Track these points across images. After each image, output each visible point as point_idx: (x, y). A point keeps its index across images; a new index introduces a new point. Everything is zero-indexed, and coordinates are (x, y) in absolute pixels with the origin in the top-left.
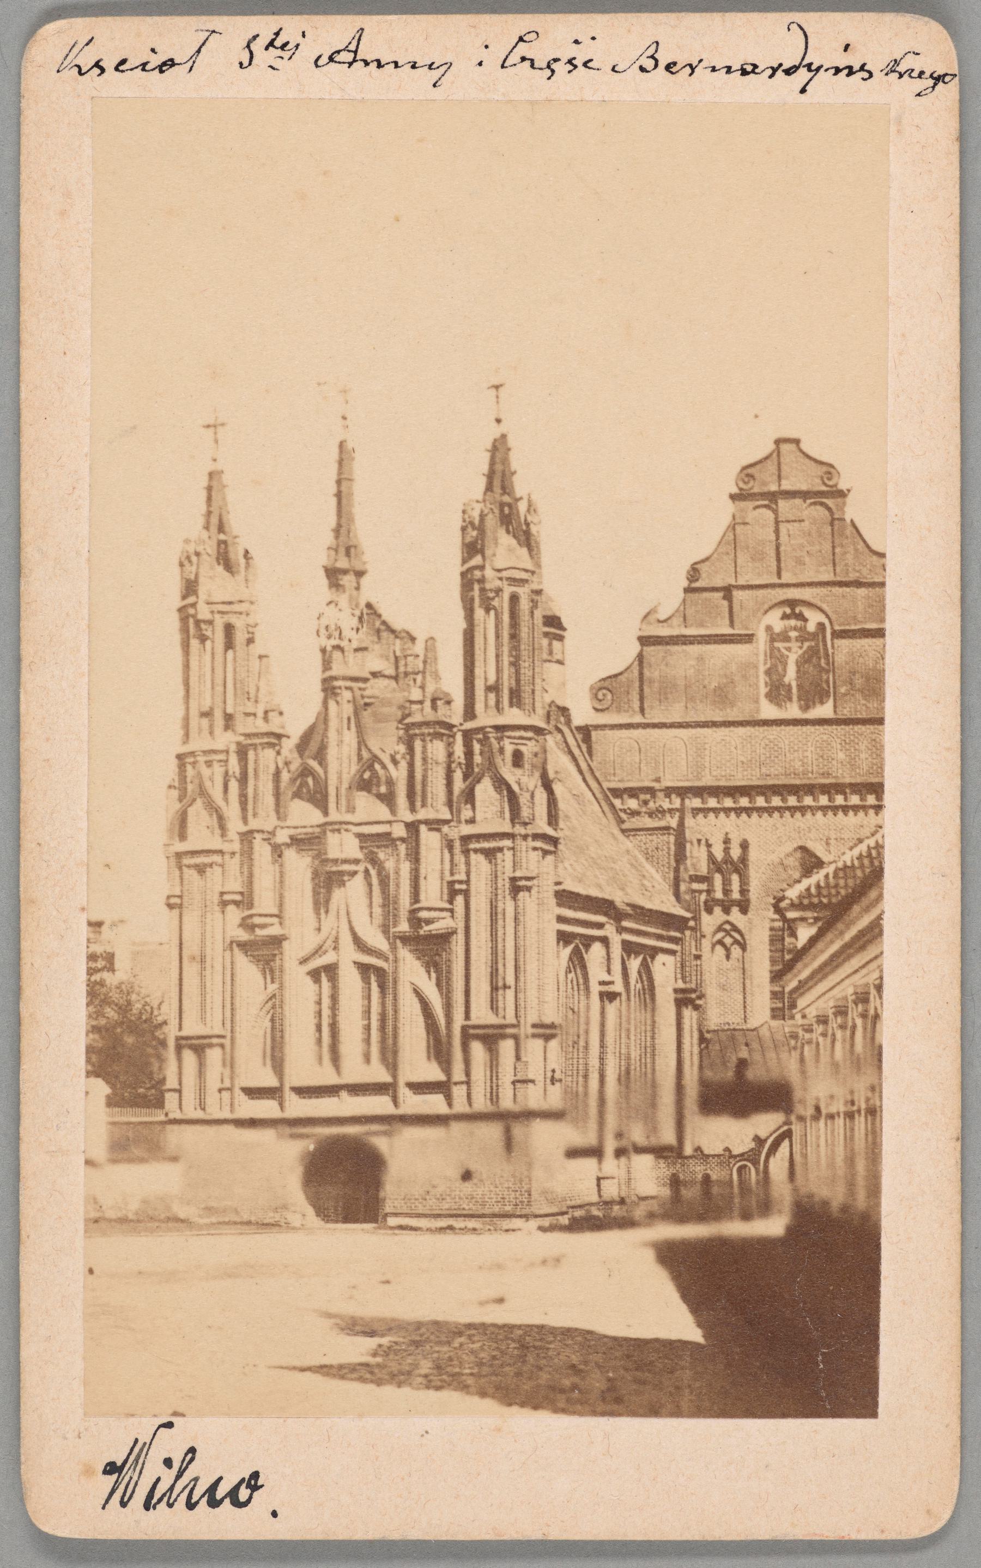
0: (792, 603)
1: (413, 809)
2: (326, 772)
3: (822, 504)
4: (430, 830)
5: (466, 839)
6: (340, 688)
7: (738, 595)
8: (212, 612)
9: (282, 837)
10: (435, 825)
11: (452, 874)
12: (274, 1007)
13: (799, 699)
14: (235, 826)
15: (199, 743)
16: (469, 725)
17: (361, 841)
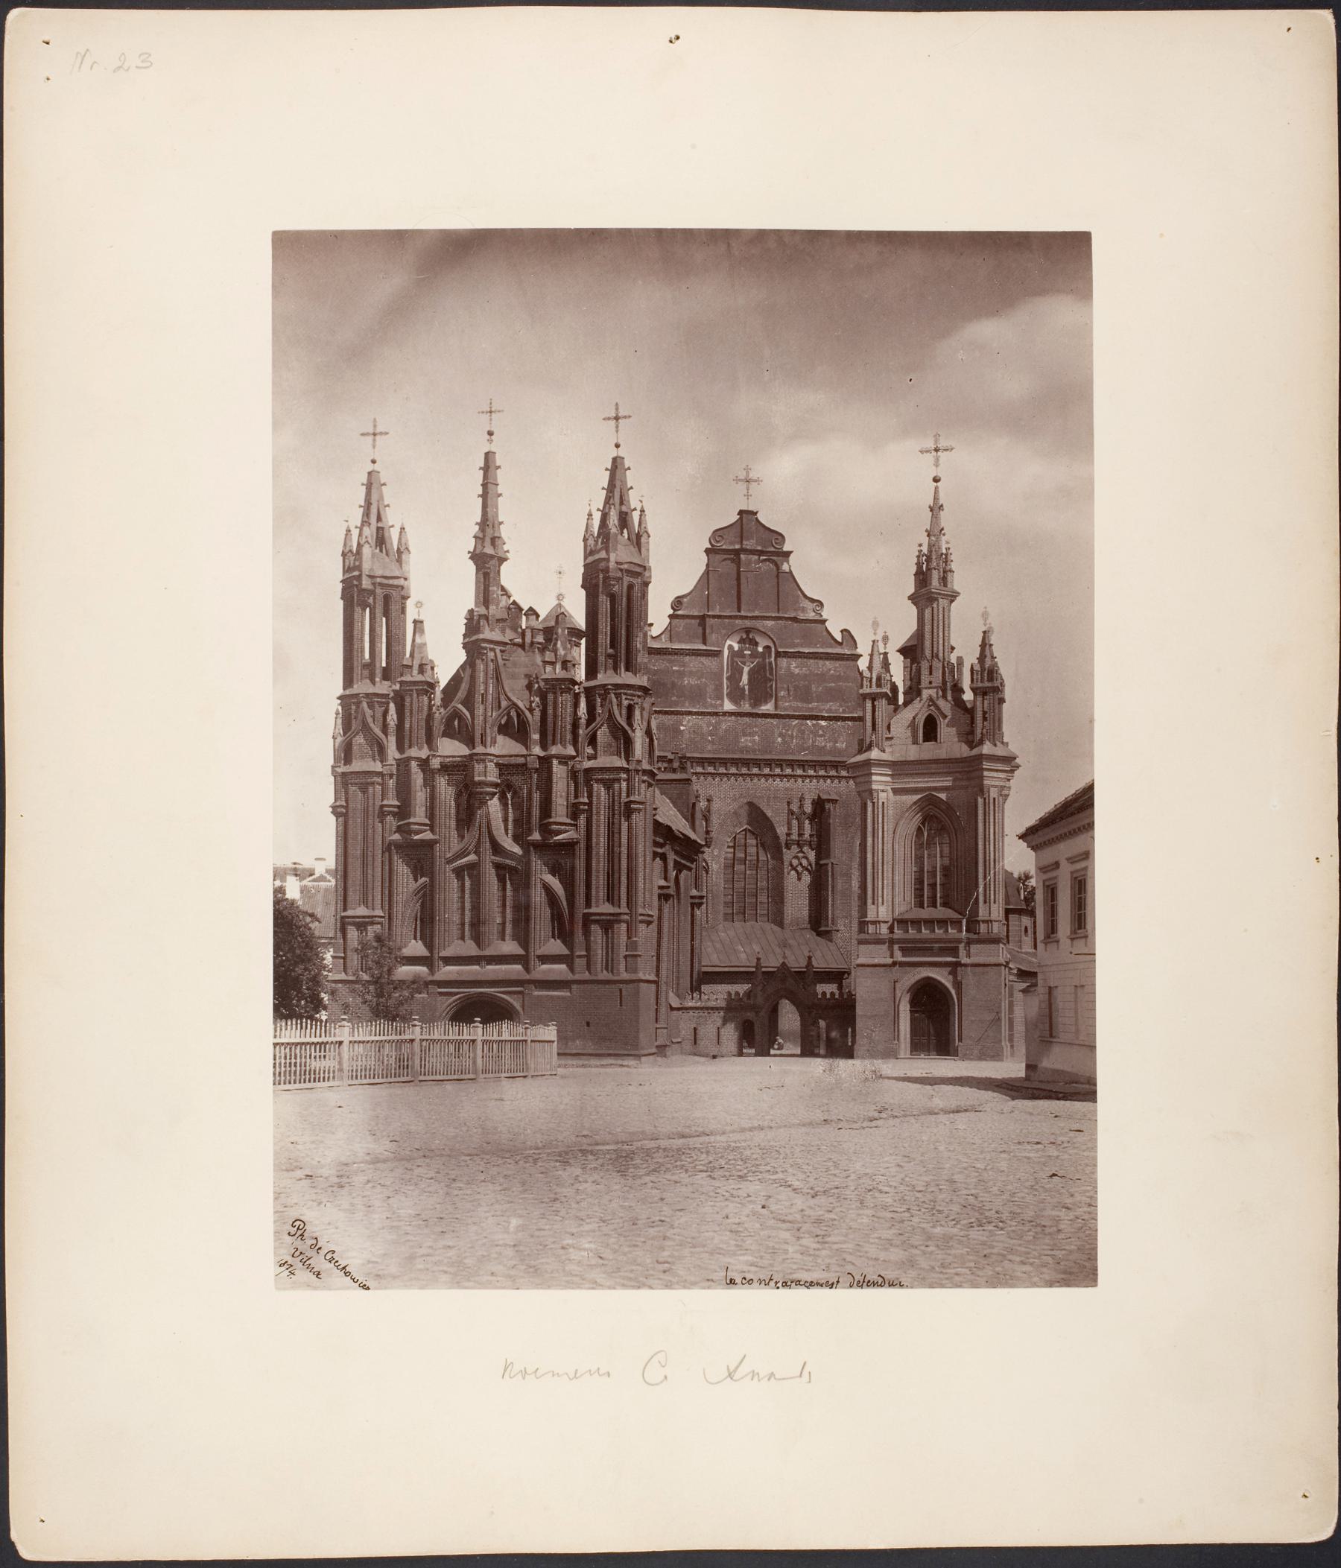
0: (748, 631)
1: (544, 747)
2: (473, 718)
4: (560, 763)
5: (587, 771)
6: (486, 648)
7: (710, 622)
8: (374, 584)
9: (435, 763)
10: (564, 760)
11: (576, 797)
12: (424, 895)
13: (750, 699)
14: (392, 752)
15: (362, 687)
16: (592, 683)
17: (500, 770)
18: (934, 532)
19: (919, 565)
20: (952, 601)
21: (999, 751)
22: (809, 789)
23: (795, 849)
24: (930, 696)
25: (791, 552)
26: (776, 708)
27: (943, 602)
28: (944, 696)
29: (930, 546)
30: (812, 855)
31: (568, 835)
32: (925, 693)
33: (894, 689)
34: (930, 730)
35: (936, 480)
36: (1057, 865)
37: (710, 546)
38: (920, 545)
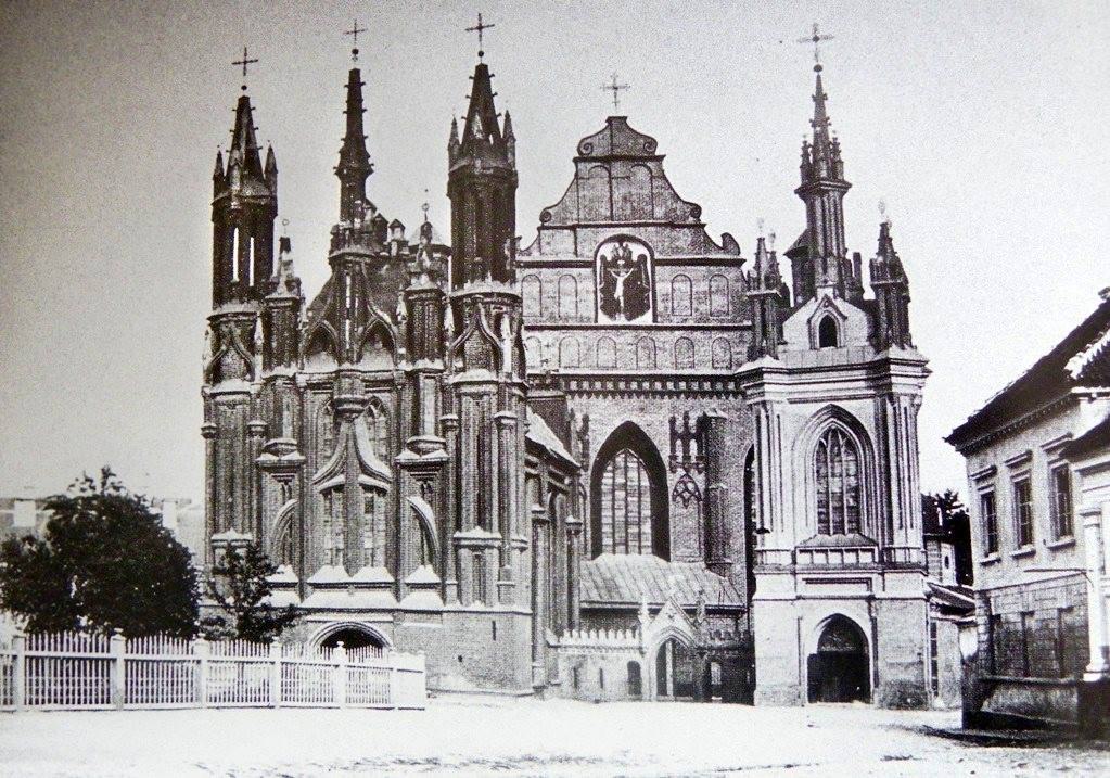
3: (645, 166)
5: (457, 385)
18: (820, 121)
19: (805, 155)
20: (843, 193)
21: (907, 354)
22: (697, 409)
23: (681, 472)
24: (826, 296)
25: (664, 156)
26: (655, 320)
27: (834, 195)
28: (842, 296)
29: (816, 136)
30: (700, 479)
31: (438, 454)
32: (821, 293)
33: (785, 289)
34: (828, 333)
35: (818, 68)
36: (994, 470)
37: (578, 155)
38: (805, 136)
